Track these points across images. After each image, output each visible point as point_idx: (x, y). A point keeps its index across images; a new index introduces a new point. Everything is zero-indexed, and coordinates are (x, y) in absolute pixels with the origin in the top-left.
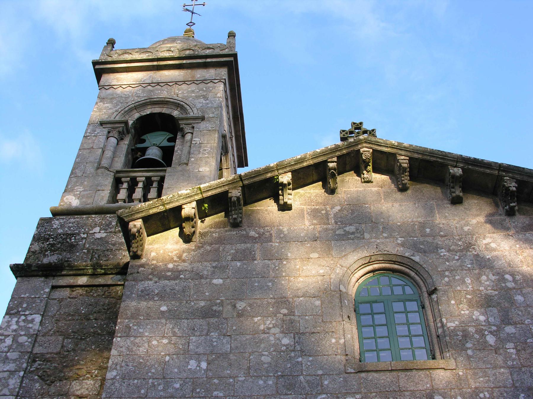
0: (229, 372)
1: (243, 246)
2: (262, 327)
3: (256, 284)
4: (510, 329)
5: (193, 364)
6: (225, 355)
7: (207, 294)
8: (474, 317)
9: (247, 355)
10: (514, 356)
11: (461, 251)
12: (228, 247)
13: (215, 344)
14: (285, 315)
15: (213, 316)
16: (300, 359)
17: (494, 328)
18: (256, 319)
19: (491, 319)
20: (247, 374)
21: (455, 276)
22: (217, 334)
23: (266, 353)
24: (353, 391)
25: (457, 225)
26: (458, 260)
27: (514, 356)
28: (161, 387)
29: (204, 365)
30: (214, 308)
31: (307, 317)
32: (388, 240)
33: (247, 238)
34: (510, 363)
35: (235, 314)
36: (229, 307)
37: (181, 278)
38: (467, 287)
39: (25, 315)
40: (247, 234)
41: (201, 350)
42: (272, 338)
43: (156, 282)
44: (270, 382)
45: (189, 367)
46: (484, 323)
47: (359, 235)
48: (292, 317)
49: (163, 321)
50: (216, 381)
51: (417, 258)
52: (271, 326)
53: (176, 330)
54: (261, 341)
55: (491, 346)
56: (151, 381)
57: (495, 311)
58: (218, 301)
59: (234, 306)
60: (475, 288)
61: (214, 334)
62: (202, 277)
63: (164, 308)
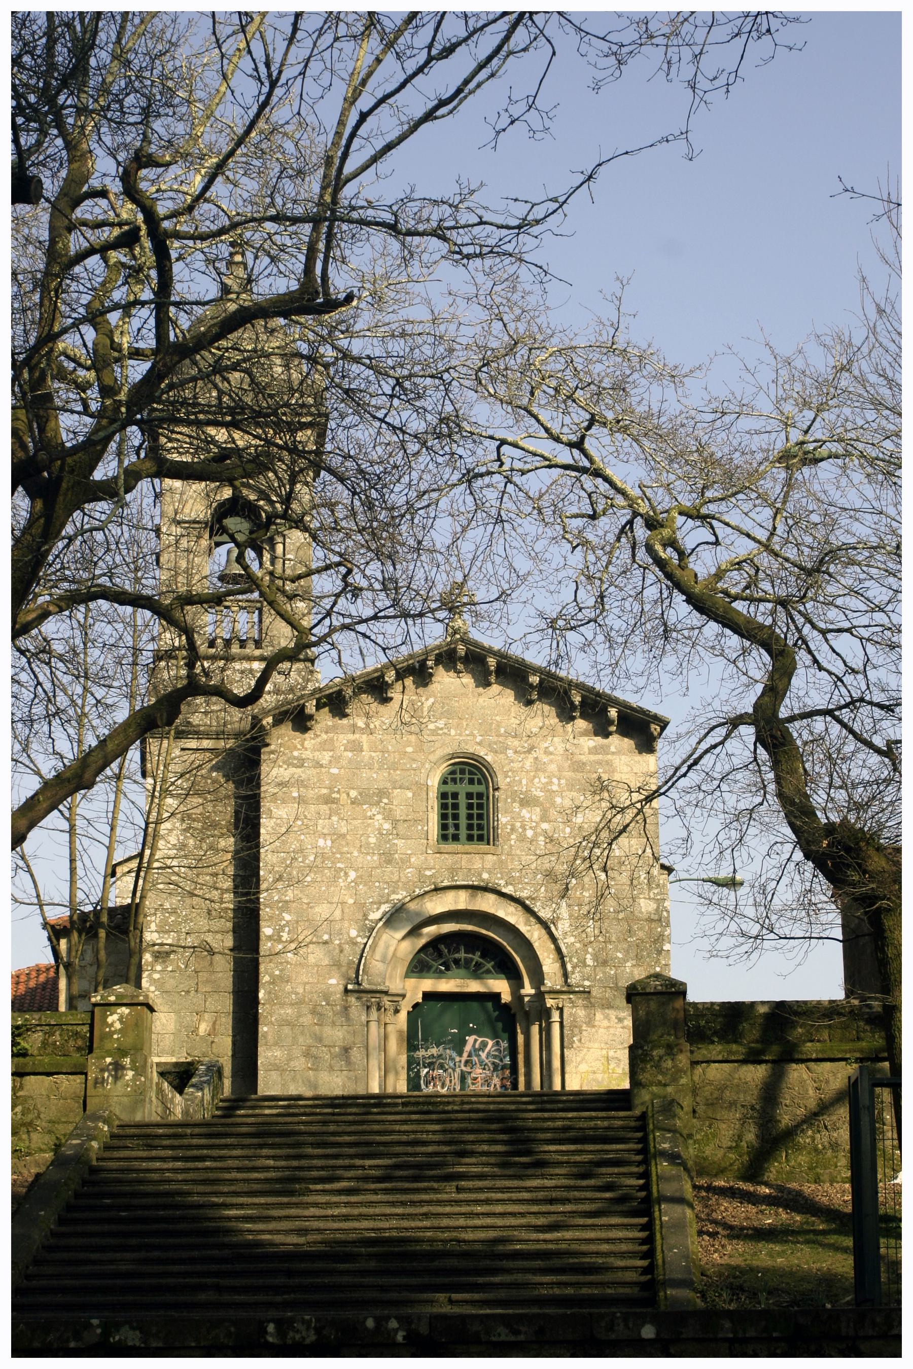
1: (351, 737)
2: (369, 814)
4: (545, 826)
5: (321, 842)
6: (343, 836)
12: (341, 736)
15: (333, 802)
19: (534, 817)
20: (360, 851)
29: (329, 843)
30: (333, 796)
33: (354, 729)
41: (325, 831)
44: (375, 858)
50: (338, 856)
51: (489, 758)
54: (369, 825)
57: (538, 809)
59: (348, 794)
61: (335, 818)
62: (321, 766)
63: (295, 794)
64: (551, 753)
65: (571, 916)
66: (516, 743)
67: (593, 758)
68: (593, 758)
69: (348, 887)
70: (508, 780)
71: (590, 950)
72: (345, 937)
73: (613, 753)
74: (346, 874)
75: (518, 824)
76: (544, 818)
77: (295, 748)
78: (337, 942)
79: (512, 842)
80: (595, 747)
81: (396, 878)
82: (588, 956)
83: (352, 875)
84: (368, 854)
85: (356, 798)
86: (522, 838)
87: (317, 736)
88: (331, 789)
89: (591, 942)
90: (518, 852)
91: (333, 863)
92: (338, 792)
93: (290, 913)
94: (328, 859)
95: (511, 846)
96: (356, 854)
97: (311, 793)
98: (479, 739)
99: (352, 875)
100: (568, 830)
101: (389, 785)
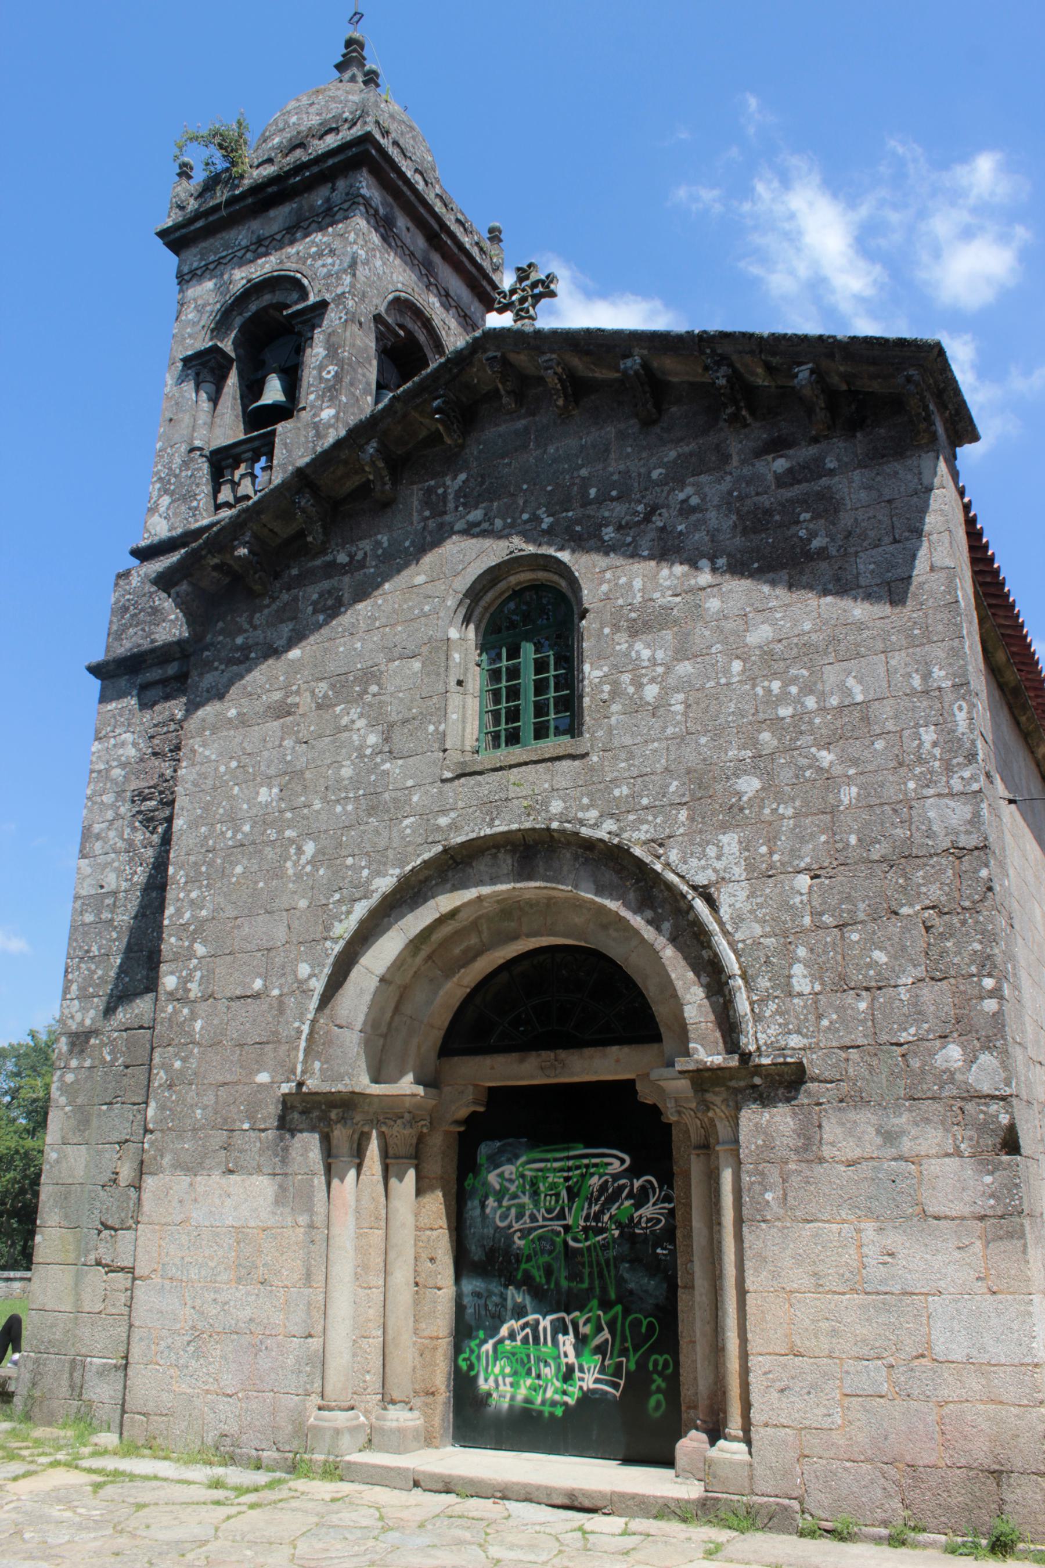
0: (303, 799)
1: (326, 585)
2: (345, 721)
3: (341, 649)
4: (685, 668)
5: (264, 795)
7: (282, 678)
8: (633, 654)
9: (324, 769)
10: (679, 717)
11: (639, 523)
12: (309, 589)
13: (289, 758)
14: (374, 695)
15: (289, 714)
16: (387, 766)
17: (660, 670)
18: (338, 709)
19: (660, 655)
20: (325, 800)
21: (619, 578)
22: (292, 743)
23: (349, 763)
24: (448, 807)
25: (642, 470)
26: (629, 544)
27: (679, 717)
28: (229, 834)
30: (289, 701)
31: (401, 695)
32: (528, 527)
34: (670, 731)
35: (313, 705)
36: (308, 694)
37: (253, 659)
38: (634, 597)
39: (115, 737)
40: (335, 560)
41: (272, 772)
42: (355, 737)
43: (223, 671)
45: (259, 799)
46: (646, 664)
47: (485, 526)
48: (382, 698)
49: (232, 732)
52: (355, 717)
53: (245, 745)
55: (649, 704)
56: (219, 826)
58: (294, 688)
59: (313, 692)
60: (647, 597)
64: (694, 510)
65: (750, 867)
66: (619, 510)
67: (787, 493)
68: (787, 493)
69: (298, 876)
70: (605, 587)
71: (802, 952)
72: (290, 979)
73: (831, 473)
74: (300, 851)
75: (626, 678)
76: (682, 653)
77: (241, 631)
78: (276, 992)
79: (613, 720)
80: (790, 471)
81: (382, 843)
82: (798, 969)
83: (310, 848)
84: (338, 801)
85: (325, 696)
86: (636, 707)
87: (274, 599)
88: (286, 688)
89: (804, 931)
90: (628, 741)
91: (280, 832)
92: (298, 693)
93: (204, 942)
94: (271, 824)
95: (611, 729)
96: (317, 806)
97: (259, 706)
98: (547, 521)
99: (310, 848)
100: (737, 666)
101: (381, 658)
